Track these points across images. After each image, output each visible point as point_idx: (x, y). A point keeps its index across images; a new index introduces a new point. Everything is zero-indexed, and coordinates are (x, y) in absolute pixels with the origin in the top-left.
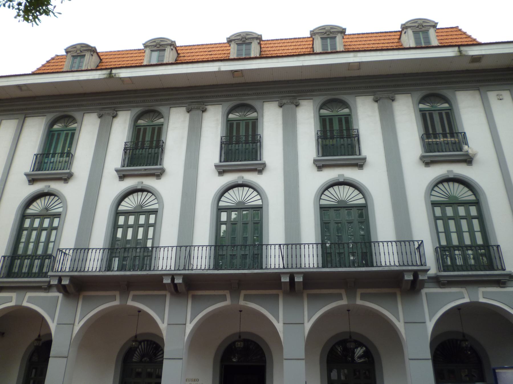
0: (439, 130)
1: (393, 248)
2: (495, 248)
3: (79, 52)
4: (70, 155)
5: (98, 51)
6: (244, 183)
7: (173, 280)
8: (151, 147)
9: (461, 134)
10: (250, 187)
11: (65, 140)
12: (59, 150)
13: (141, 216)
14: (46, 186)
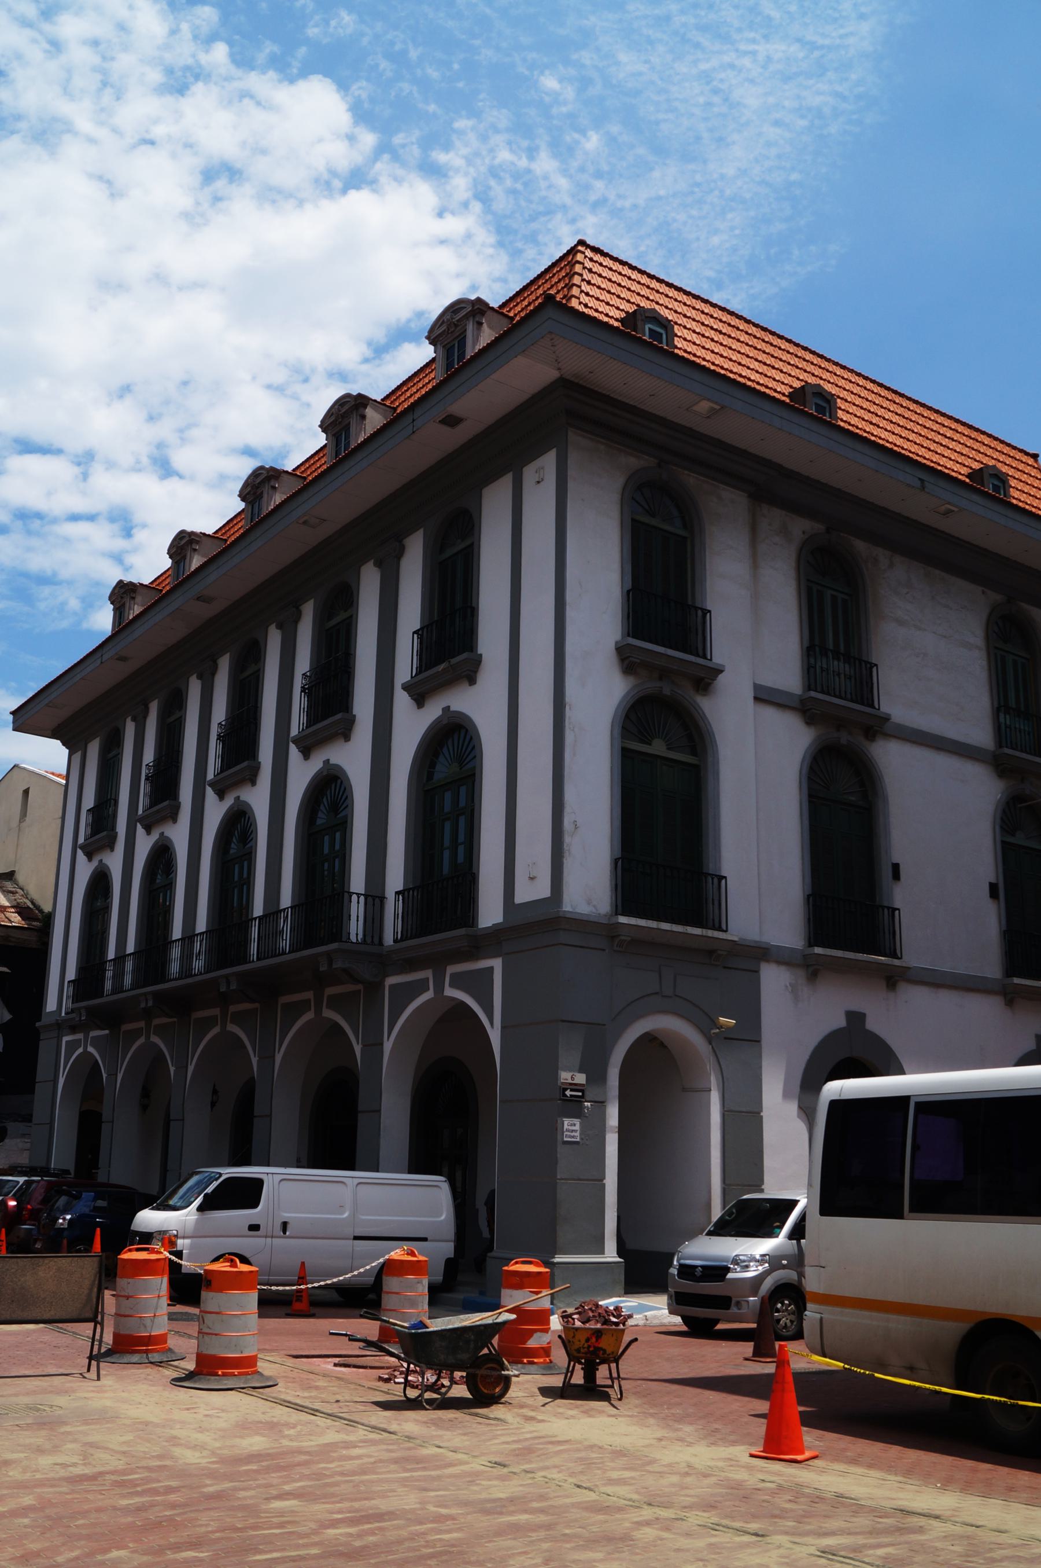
3: (120, 599)
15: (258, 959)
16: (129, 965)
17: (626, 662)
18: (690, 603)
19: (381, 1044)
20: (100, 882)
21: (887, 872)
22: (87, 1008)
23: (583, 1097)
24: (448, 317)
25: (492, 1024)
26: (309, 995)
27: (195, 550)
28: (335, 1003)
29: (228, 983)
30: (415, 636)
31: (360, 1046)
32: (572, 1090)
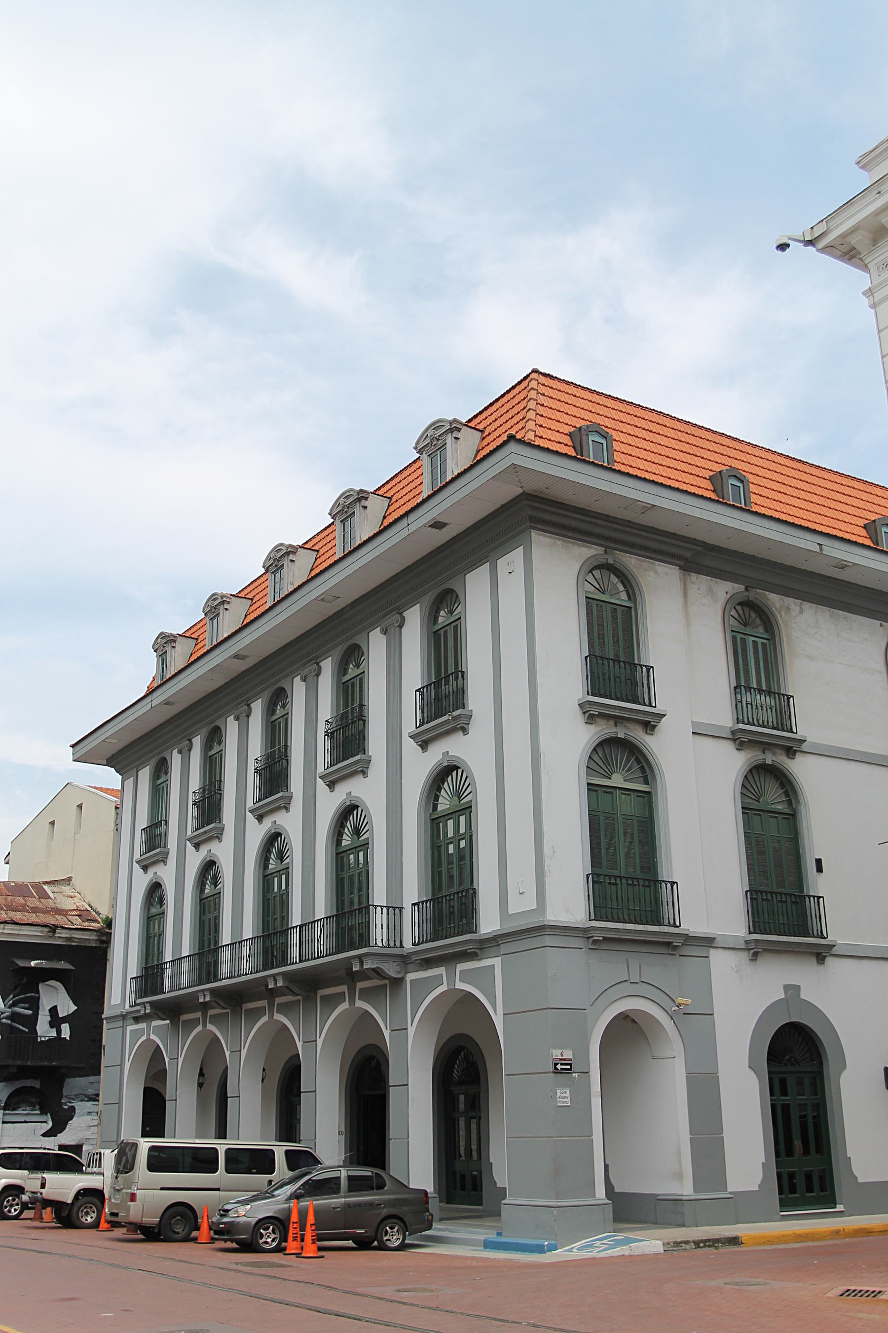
3: (162, 648)
15: (301, 961)
16: (185, 966)
17: (587, 715)
18: (636, 662)
20: (155, 890)
21: (811, 866)
22: (150, 1002)
23: (571, 1069)
24: (430, 432)
25: (495, 1012)
26: (344, 988)
27: (227, 609)
28: (366, 994)
29: (276, 981)
30: (418, 693)
31: (389, 1031)
32: (562, 1064)
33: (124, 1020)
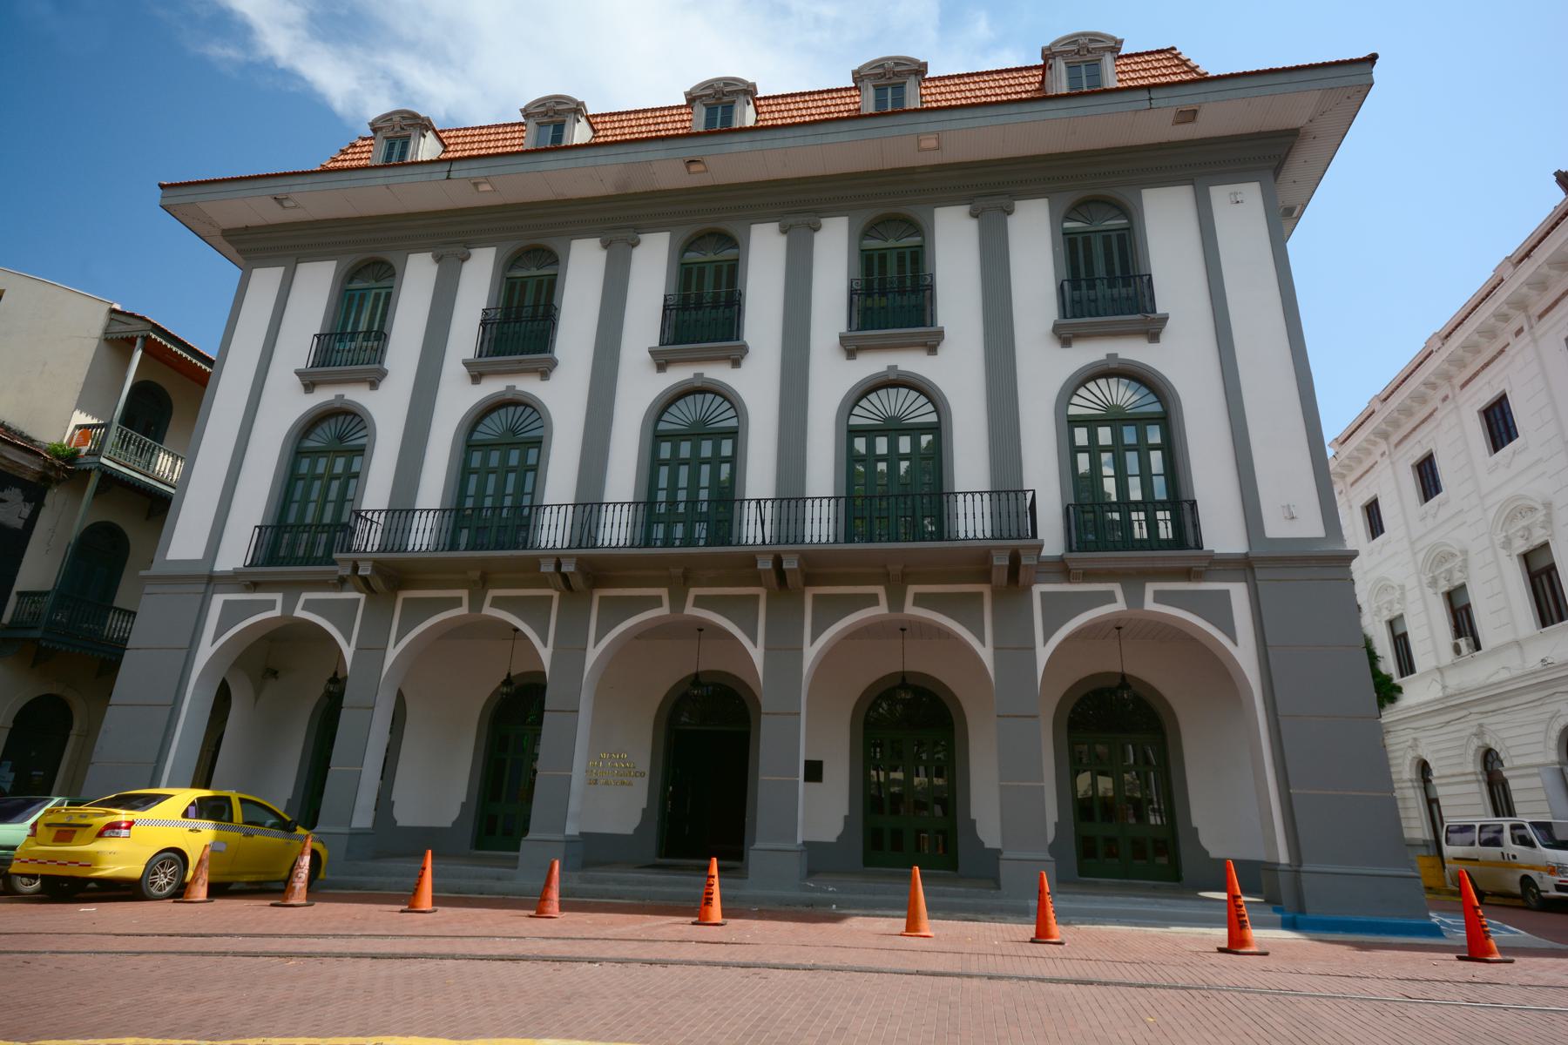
0: (1100, 269)
1: (983, 506)
2: (1186, 506)
3: (397, 129)
4: (380, 336)
5: (437, 129)
6: (705, 385)
7: (558, 566)
8: (534, 318)
9: (1142, 279)
10: (716, 393)
11: (375, 307)
12: (363, 326)
13: (512, 451)
14: (337, 396)
19: (1032, 648)
24: (1082, 40)
33: (208, 584)
